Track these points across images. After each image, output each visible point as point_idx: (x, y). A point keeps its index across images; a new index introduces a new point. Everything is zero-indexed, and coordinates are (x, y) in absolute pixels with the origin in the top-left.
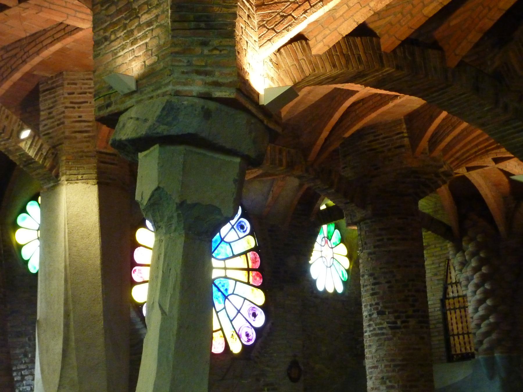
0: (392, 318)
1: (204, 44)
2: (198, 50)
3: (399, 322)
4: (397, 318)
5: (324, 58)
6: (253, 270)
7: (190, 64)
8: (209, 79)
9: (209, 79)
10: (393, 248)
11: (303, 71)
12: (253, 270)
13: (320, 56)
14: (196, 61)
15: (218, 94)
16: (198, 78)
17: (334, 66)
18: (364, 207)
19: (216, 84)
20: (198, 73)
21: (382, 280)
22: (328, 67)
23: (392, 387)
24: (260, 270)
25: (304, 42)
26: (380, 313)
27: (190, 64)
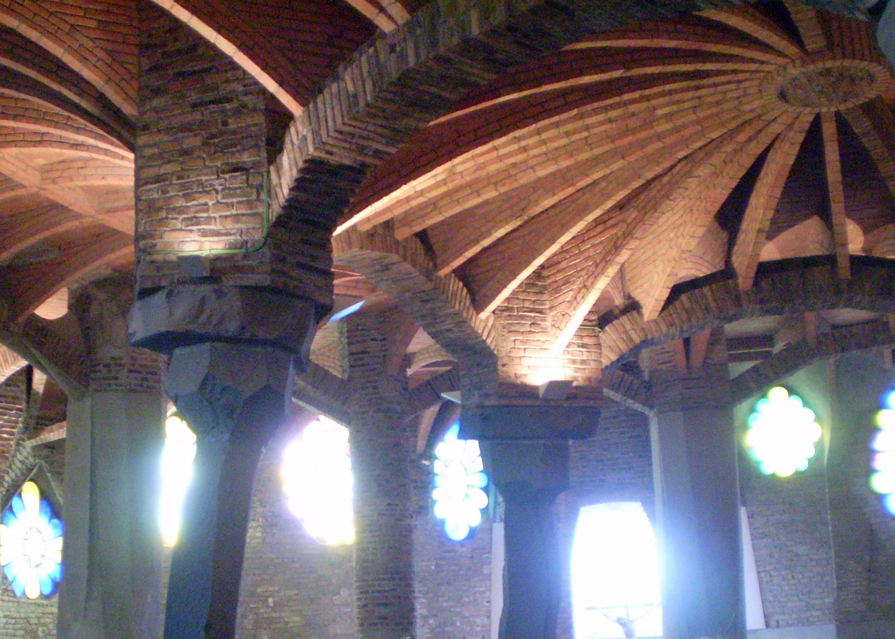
1: (479, 365)
5: (660, 320)
13: (655, 321)
14: (475, 380)
15: (487, 403)
16: (476, 393)
19: (487, 396)
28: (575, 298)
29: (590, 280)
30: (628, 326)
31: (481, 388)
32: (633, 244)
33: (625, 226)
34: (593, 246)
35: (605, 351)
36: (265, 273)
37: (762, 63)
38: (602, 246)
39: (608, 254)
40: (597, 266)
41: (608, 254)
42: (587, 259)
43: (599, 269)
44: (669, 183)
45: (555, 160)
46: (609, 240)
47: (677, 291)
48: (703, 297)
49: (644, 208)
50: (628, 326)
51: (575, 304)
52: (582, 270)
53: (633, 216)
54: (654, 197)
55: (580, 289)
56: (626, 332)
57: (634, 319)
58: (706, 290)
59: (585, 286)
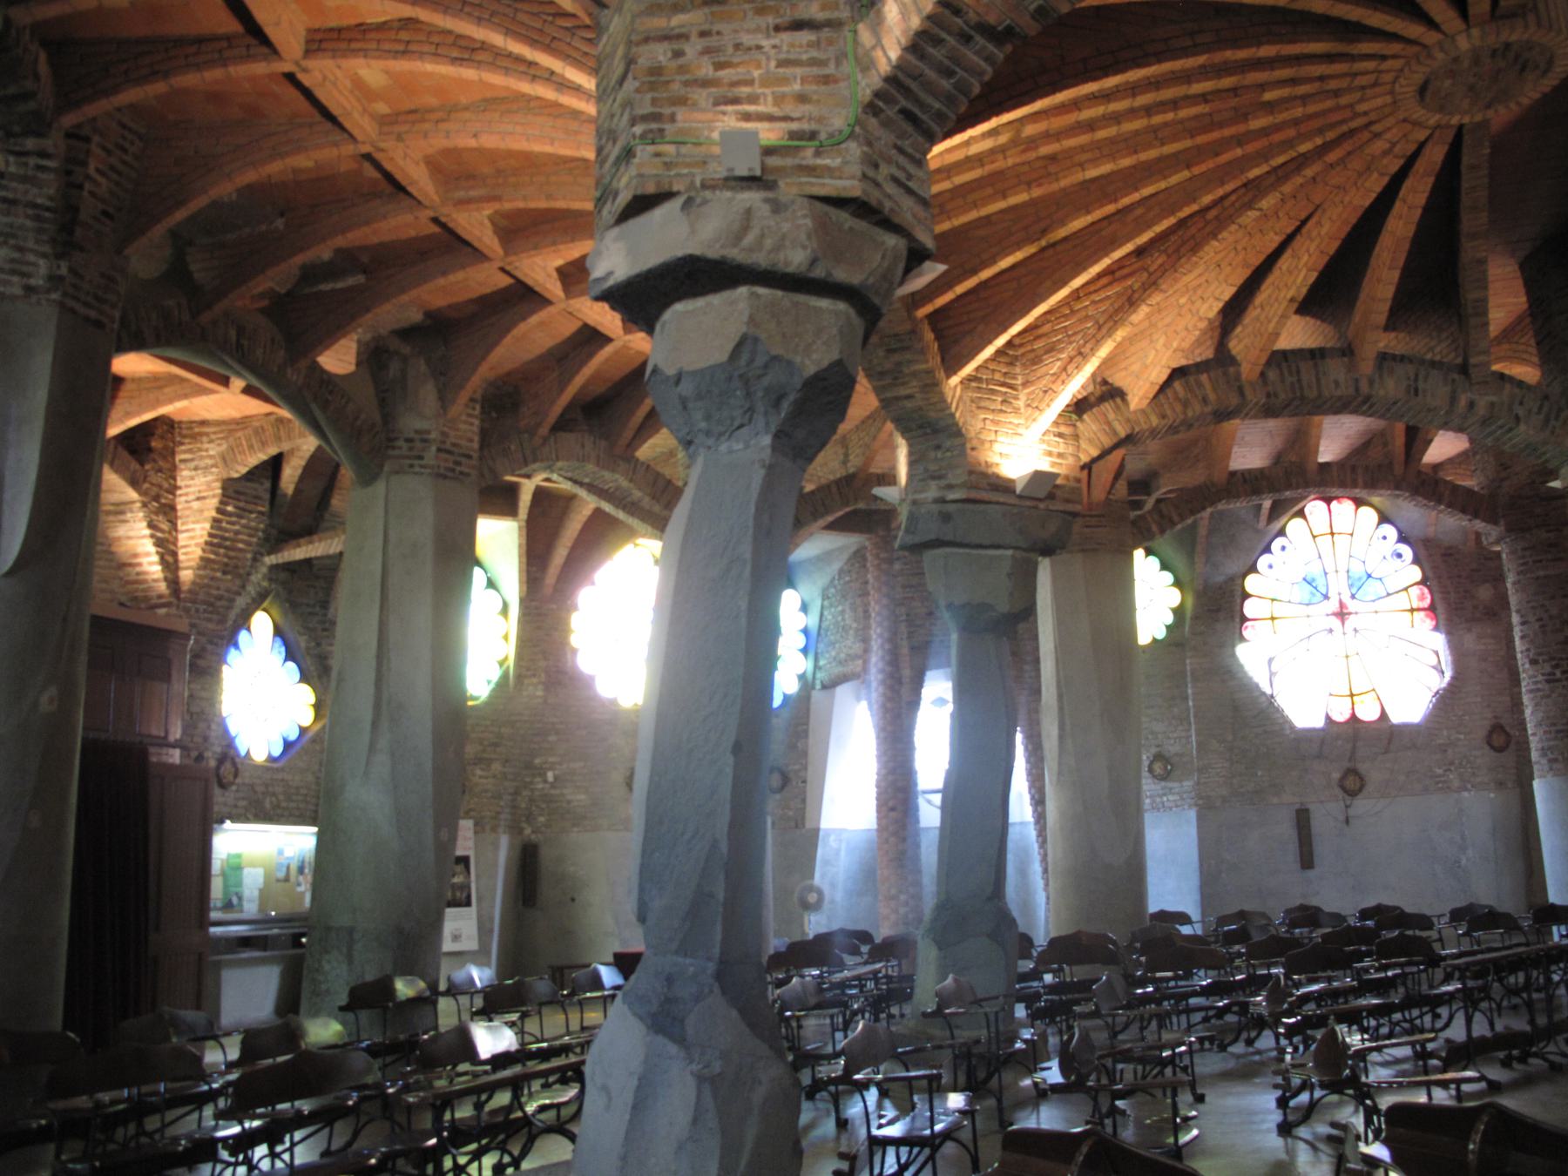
0: (1547, 668)
1: (938, 447)
2: (932, 454)
3: (1558, 674)
4: (1557, 666)
5: (1149, 411)
6: (1419, 610)
7: (926, 470)
8: (943, 482)
9: (943, 482)
10: (1541, 573)
11: (1115, 433)
12: (1419, 610)
13: (1143, 411)
14: (932, 467)
15: (951, 496)
16: (933, 484)
17: (1164, 417)
18: (1495, 523)
19: (950, 487)
20: (933, 478)
21: (1532, 619)
22: (1155, 421)
23: (1555, 760)
24: (1432, 609)
25: (1118, 400)
26: (1533, 662)
27: (926, 470)
28: (1065, 369)
29: (1089, 345)
30: (1111, 416)
31: (940, 477)
32: (1156, 298)
33: (1145, 275)
34: (1094, 302)
35: (1084, 445)
36: (853, 177)
37: (1384, 58)
38: (1108, 303)
39: (1117, 311)
40: (1100, 328)
41: (1117, 311)
42: (1087, 318)
43: (1104, 331)
44: (1216, 217)
45: (1112, 157)
46: (1118, 295)
47: (1177, 373)
48: (1200, 385)
49: (1177, 250)
50: (1111, 416)
51: (1064, 376)
52: (1075, 334)
53: (1159, 261)
54: (1193, 236)
55: (1071, 359)
56: (1109, 423)
57: (1118, 407)
58: (1204, 378)
59: (1080, 353)
